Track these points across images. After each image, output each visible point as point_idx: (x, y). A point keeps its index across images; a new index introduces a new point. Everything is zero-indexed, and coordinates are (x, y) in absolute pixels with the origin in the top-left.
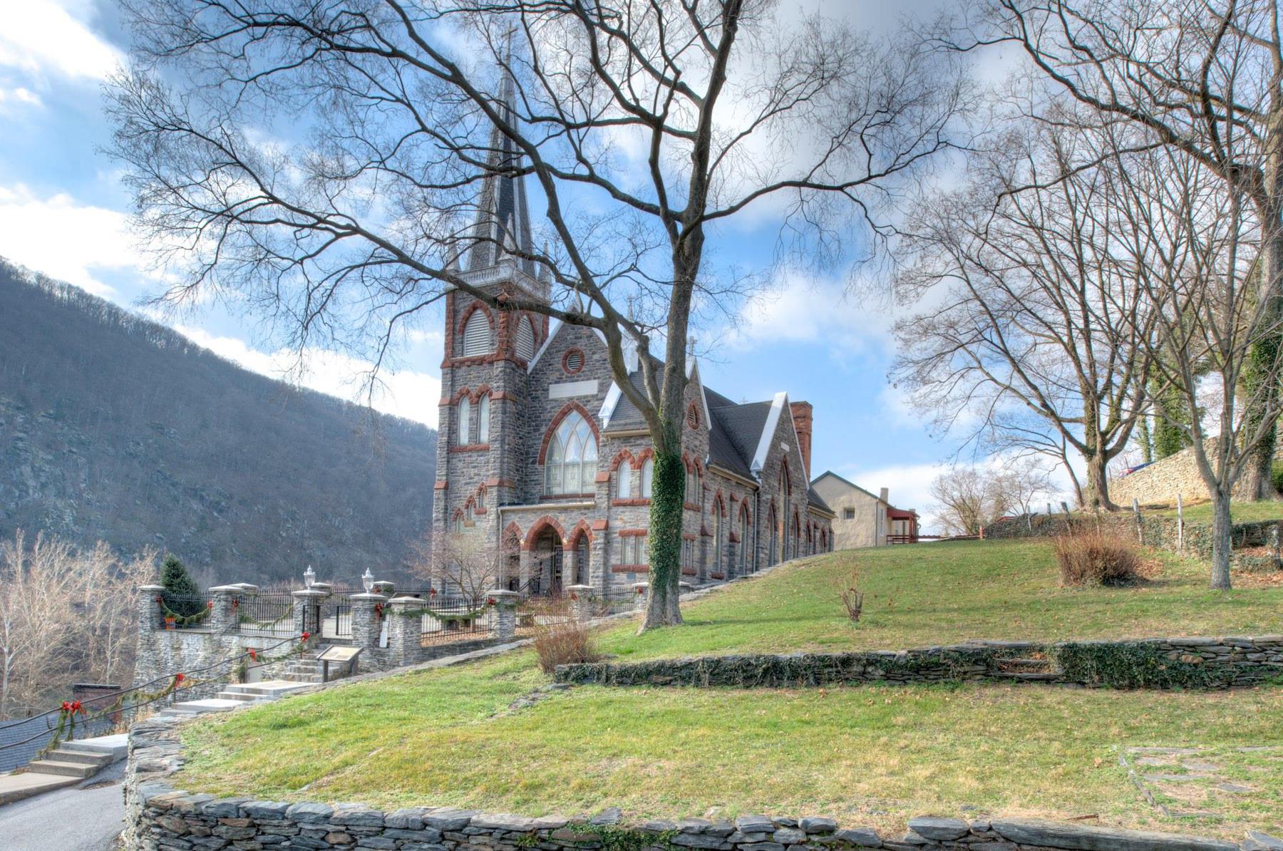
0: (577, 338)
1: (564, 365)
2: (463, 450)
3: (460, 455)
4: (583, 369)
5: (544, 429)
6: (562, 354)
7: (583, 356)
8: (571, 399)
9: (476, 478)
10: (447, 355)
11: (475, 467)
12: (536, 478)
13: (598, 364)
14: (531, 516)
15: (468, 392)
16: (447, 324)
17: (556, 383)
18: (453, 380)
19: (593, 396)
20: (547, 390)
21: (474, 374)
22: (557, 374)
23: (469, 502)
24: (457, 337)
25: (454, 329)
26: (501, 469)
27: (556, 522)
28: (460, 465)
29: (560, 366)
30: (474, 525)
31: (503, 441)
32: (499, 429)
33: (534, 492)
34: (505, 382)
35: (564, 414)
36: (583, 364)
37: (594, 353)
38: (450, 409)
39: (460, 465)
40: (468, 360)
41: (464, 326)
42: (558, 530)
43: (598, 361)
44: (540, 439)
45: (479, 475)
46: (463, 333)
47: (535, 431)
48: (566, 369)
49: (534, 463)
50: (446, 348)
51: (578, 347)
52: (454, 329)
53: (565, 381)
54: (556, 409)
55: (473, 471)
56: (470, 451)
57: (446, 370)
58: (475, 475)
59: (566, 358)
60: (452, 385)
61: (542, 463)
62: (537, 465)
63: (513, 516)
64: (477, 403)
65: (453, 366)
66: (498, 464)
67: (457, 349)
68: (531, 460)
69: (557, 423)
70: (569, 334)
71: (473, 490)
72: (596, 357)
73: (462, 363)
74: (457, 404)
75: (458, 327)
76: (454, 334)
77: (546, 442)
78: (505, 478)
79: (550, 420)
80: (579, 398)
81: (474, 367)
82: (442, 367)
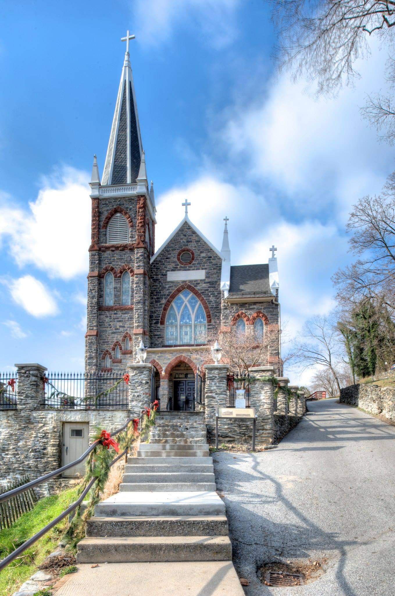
0: (188, 242)
1: (179, 259)
2: (109, 309)
3: (107, 313)
4: (194, 262)
5: (164, 301)
6: (177, 252)
7: (193, 254)
8: (184, 282)
9: (121, 329)
10: (93, 242)
11: (120, 321)
12: (158, 333)
13: (204, 260)
14: (168, 356)
15: (112, 269)
16: (93, 221)
17: (172, 270)
18: (100, 260)
19: (201, 280)
20: (166, 275)
21: (117, 257)
22: (173, 265)
23: (115, 345)
24: (102, 230)
25: (99, 225)
26: (144, 322)
27: (189, 360)
28: (107, 320)
29: (176, 259)
30: (120, 362)
31: (144, 303)
32: (142, 295)
33: (157, 343)
34: (144, 263)
35: (179, 291)
36: (193, 259)
37: (201, 252)
38: (98, 280)
39: (107, 320)
40: (112, 246)
41: (107, 223)
42: (191, 365)
43: (204, 257)
44: (161, 307)
45: (124, 327)
46: (106, 228)
47: (156, 302)
48: (180, 262)
49: (157, 323)
50: (93, 237)
51: (189, 247)
52: (99, 225)
53: (180, 270)
54: (174, 288)
55: (119, 324)
56: (116, 310)
57: (94, 252)
58: (120, 327)
59: (179, 255)
60: (99, 264)
61: (162, 323)
62: (159, 325)
63: (153, 356)
64: (120, 277)
65: (100, 250)
66: (141, 320)
67: (102, 239)
68: (154, 321)
69: (173, 296)
70: (182, 239)
71: (120, 338)
72: (203, 255)
73: (108, 248)
74: (103, 277)
75: (102, 224)
76: (99, 228)
77: (165, 309)
78: (146, 329)
79: (168, 295)
80: (191, 281)
81: (117, 252)
82: (90, 250)
